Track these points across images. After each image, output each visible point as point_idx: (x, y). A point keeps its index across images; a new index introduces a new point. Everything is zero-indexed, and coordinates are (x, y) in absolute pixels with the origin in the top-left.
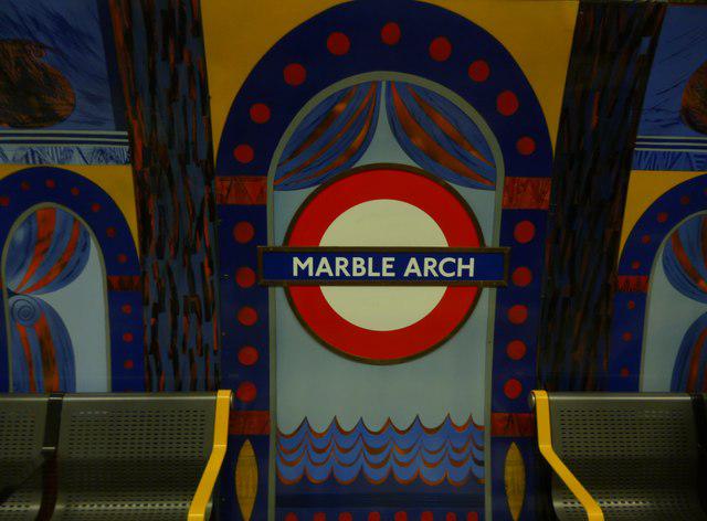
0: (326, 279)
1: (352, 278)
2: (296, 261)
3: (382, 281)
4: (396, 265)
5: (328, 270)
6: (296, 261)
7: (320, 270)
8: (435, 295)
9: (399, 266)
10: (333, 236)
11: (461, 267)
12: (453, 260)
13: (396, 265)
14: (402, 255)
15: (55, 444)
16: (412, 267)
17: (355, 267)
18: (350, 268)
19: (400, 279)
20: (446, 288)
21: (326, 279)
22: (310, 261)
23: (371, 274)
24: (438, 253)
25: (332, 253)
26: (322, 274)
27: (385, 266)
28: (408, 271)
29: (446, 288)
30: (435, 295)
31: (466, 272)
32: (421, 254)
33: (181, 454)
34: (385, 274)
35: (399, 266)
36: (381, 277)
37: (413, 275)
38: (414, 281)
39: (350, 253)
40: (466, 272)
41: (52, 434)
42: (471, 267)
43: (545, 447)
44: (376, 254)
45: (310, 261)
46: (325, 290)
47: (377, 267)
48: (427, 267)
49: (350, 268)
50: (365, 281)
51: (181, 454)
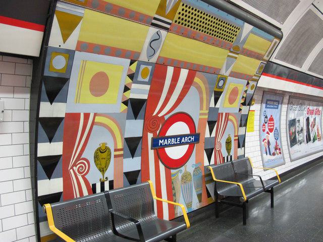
0: (166, 146)
1: (171, 144)
4: (179, 140)
7: (165, 143)
8: (187, 147)
9: (180, 141)
10: (168, 134)
13: (179, 140)
14: (181, 136)
18: (171, 142)
19: (181, 144)
20: (188, 146)
27: (178, 140)
29: (188, 146)
30: (187, 147)
32: (185, 136)
34: (178, 143)
36: (177, 144)
39: (171, 137)
43: (215, 179)
44: (175, 137)
47: (176, 141)
48: (186, 140)
49: (171, 142)
50: (174, 145)
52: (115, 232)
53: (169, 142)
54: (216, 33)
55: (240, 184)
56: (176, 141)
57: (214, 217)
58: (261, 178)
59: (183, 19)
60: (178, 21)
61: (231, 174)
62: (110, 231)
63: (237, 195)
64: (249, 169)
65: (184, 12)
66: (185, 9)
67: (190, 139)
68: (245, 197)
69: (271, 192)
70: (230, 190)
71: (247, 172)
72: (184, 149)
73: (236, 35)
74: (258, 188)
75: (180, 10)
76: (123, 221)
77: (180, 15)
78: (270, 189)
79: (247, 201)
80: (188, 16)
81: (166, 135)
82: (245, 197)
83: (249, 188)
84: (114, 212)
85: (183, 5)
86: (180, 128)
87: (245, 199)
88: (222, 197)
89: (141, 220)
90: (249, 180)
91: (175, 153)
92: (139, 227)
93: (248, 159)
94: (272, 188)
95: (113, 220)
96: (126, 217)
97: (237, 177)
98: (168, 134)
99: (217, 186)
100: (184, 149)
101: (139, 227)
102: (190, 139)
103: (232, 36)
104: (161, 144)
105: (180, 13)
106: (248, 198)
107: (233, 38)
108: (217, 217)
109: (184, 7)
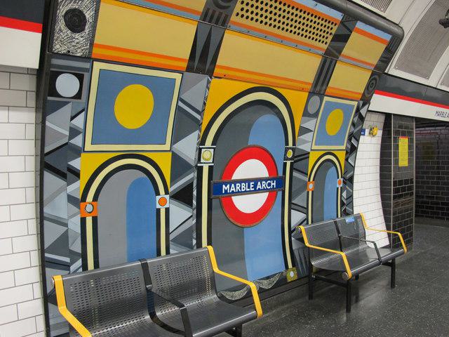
0: (234, 193)
2: (224, 186)
3: (251, 192)
4: (253, 185)
5: (234, 189)
6: (224, 186)
7: (232, 190)
8: (266, 194)
9: (255, 186)
11: (272, 184)
12: (269, 182)
13: (253, 185)
14: (256, 181)
15: (147, 289)
16: (259, 186)
17: (242, 187)
18: (241, 188)
19: (256, 191)
21: (234, 193)
22: (228, 186)
23: (248, 190)
24: (266, 180)
25: (235, 182)
26: (233, 191)
27: (252, 186)
28: (258, 187)
30: (266, 194)
31: (273, 186)
32: (261, 180)
33: (173, 284)
34: (251, 189)
35: (255, 186)
36: (250, 191)
37: (259, 189)
38: (259, 191)
39: (241, 181)
40: (273, 186)
41: (147, 279)
42: (275, 184)
44: (247, 181)
45: (228, 186)
47: (249, 187)
48: (263, 185)
49: (241, 188)
50: (245, 193)
51: (173, 284)
52: (153, 315)
53: (237, 188)
56: (249, 187)
57: (307, 298)
58: (375, 244)
62: (148, 317)
67: (269, 185)
68: (350, 273)
69: (391, 264)
70: (330, 262)
71: (357, 236)
73: (331, 34)
74: (373, 257)
76: (163, 302)
78: (390, 261)
79: (356, 276)
81: (233, 179)
82: (350, 273)
88: (320, 271)
89: (190, 304)
90: (360, 247)
93: (359, 217)
95: (150, 301)
96: (166, 297)
97: (340, 245)
98: (236, 176)
99: (309, 254)
102: (269, 185)
103: (325, 34)
104: (226, 191)
108: (311, 297)
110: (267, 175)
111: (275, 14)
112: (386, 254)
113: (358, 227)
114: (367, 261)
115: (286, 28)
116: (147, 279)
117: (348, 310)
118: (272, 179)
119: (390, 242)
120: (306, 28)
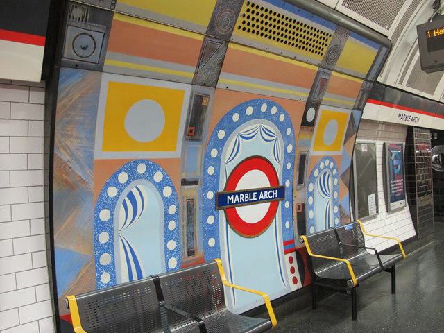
1: (245, 202)
5: (238, 200)
7: (236, 200)
8: (267, 206)
9: (258, 196)
10: (239, 187)
11: (274, 194)
13: (256, 195)
14: (259, 191)
17: (246, 197)
19: (259, 201)
23: (251, 200)
24: (268, 190)
25: (239, 193)
28: (260, 197)
32: (263, 190)
34: (254, 199)
35: (258, 196)
38: (262, 201)
39: (244, 192)
41: (161, 298)
42: (276, 193)
43: (310, 254)
44: (251, 192)
46: (239, 210)
47: (252, 198)
48: (265, 195)
50: (249, 203)
53: (241, 198)
54: (296, 39)
55: (347, 261)
56: (252, 198)
58: (376, 251)
59: (253, 25)
60: (242, 26)
61: (334, 245)
63: (343, 277)
64: (360, 237)
65: (250, 14)
66: (251, 9)
67: (271, 194)
68: (355, 280)
69: (391, 270)
71: (356, 242)
72: (263, 208)
73: (326, 45)
74: (374, 264)
75: (243, 11)
77: (245, 19)
79: (358, 285)
80: (260, 20)
82: (355, 280)
83: (359, 266)
84: (167, 306)
85: (248, 3)
86: (255, 179)
87: (355, 283)
88: (324, 280)
89: (205, 318)
91: (252, 214)
92: (202, 327)
94: (393, 267)
98: (239, 187)
100: (263, 208)
101: (202, 327)
102: (271, 194)
103: (321, 45)
105: (244, 15)
106: (358, 281)
107: (323, 49)
109: (249, 7)
110: (267, 184)
111: (270, 25)
112: (386, 259)
113: (356, 233)
114: (368, 268)
115: (285, 40)
116: (160, 297)
117: (354, 318)
118: (275, 190)
119: (416, 232)
120: (302, 38)
